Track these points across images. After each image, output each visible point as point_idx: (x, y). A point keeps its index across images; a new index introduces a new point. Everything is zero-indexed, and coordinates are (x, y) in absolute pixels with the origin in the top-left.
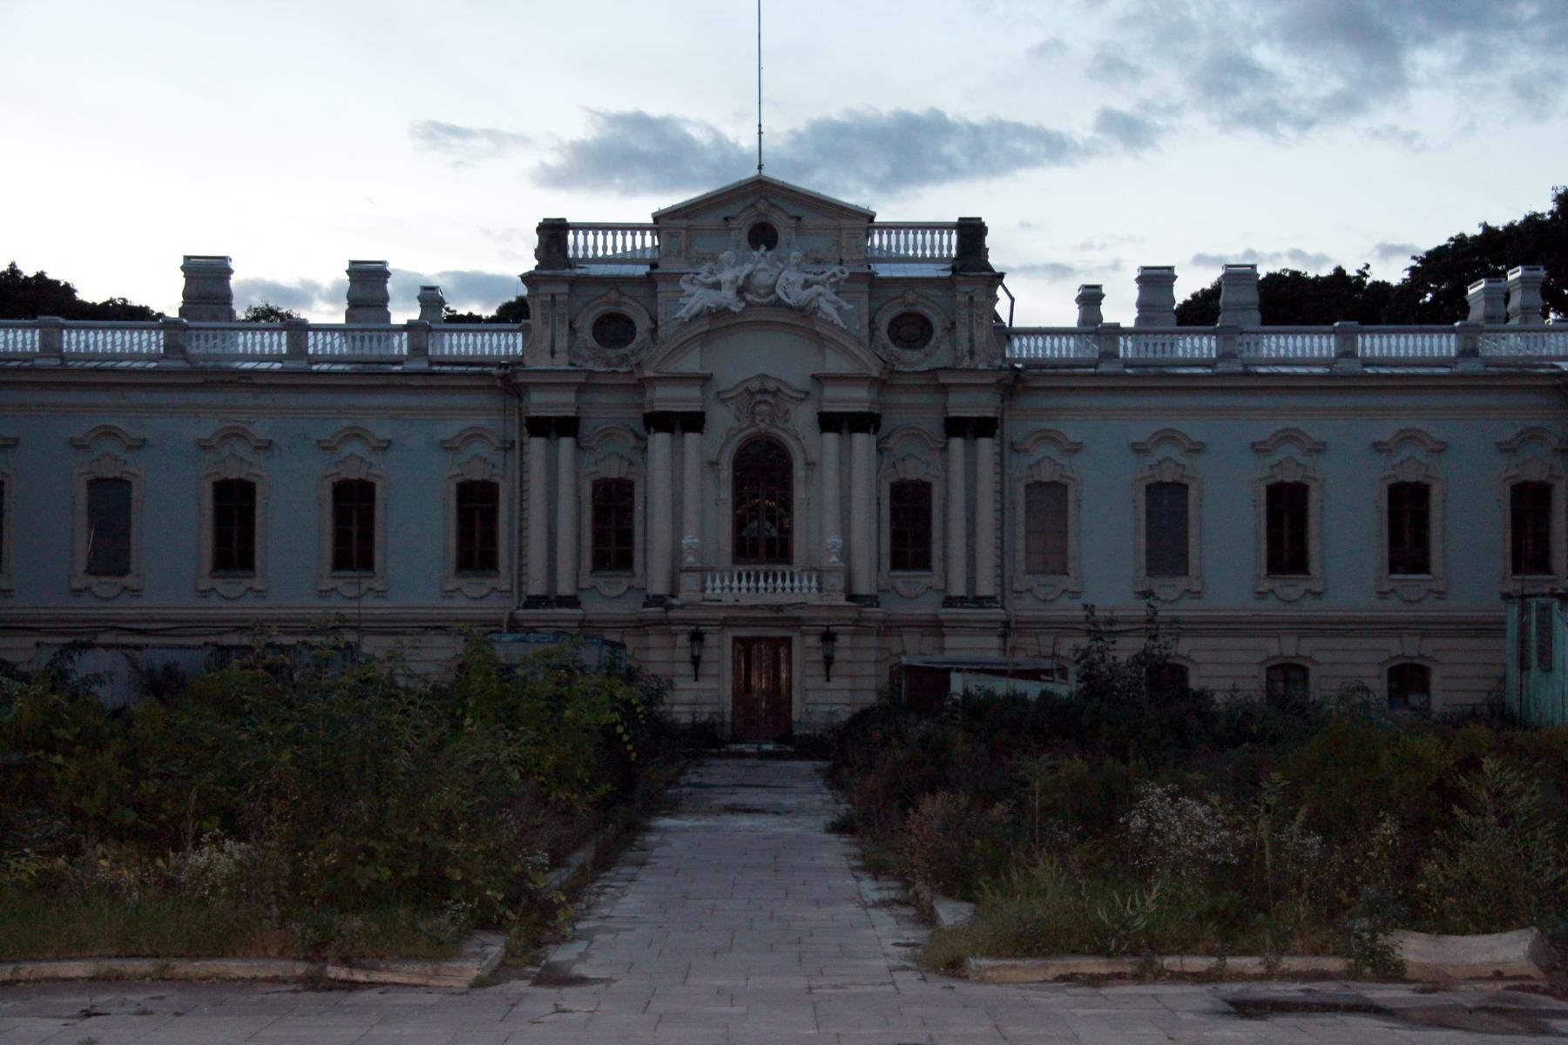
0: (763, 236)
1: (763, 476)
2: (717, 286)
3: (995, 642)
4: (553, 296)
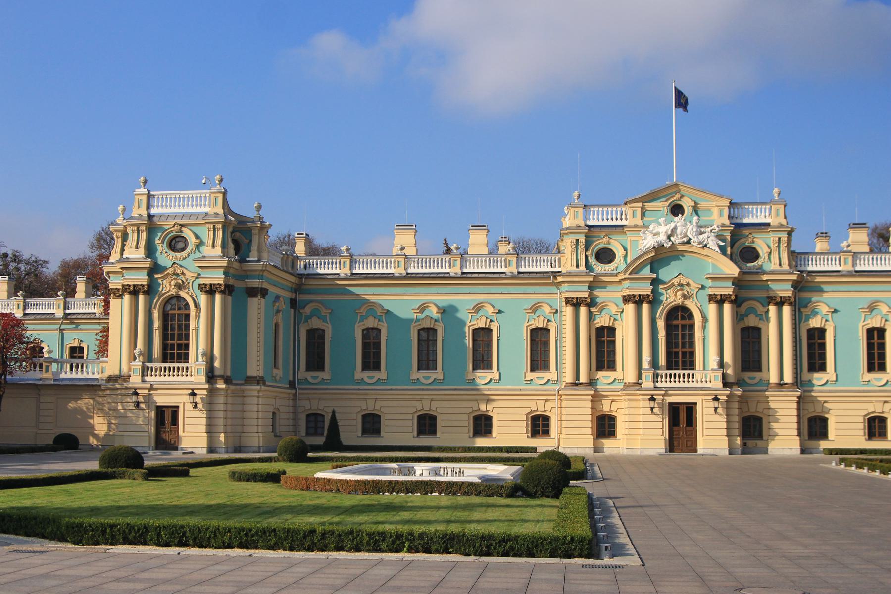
0: (676, 210)
2: (657, 234)
3: (795, 406)
4: (577, 240)
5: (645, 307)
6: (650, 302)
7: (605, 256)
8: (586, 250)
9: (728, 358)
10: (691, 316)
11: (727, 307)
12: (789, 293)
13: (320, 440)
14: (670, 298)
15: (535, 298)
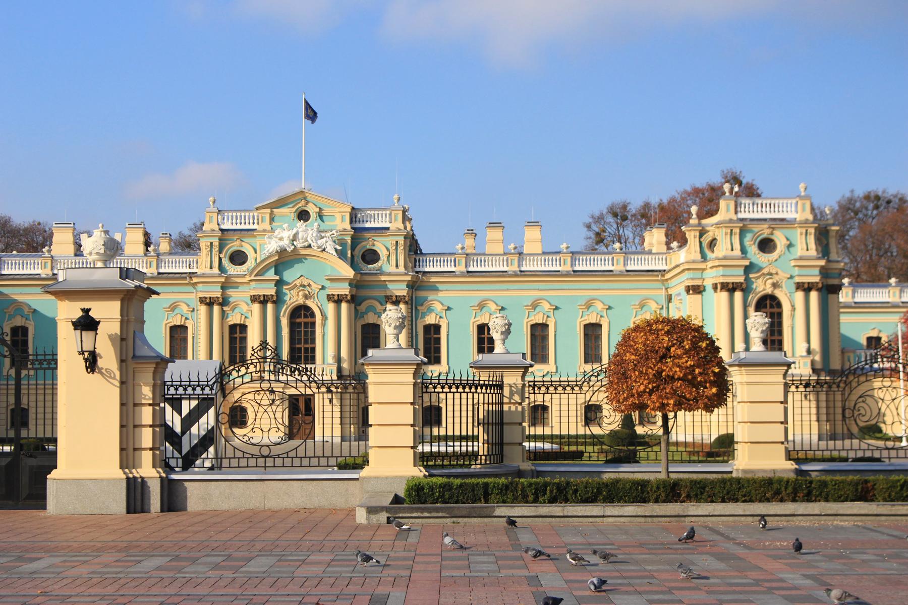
0: (303, 216)
2: (281, 239)
4: (211, 243)
5: (270, 306)
6: (274, 302)
7: (238, 258)
8: (220, 252)
9: (344, 353)
10: (313, 315)
11: (344, 306)
12: (404, 293)
14: (293, 298)
15: (173, 297)
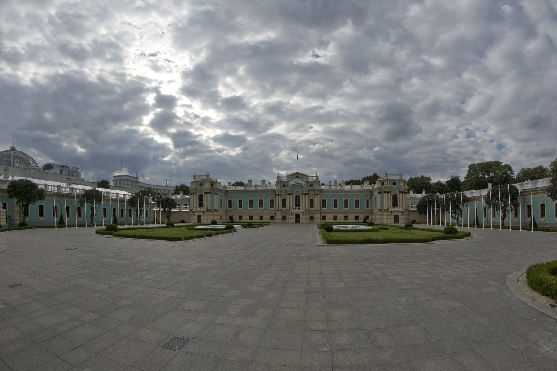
0: (298, 177)
1: (298, 199)
13: (230, 221)
